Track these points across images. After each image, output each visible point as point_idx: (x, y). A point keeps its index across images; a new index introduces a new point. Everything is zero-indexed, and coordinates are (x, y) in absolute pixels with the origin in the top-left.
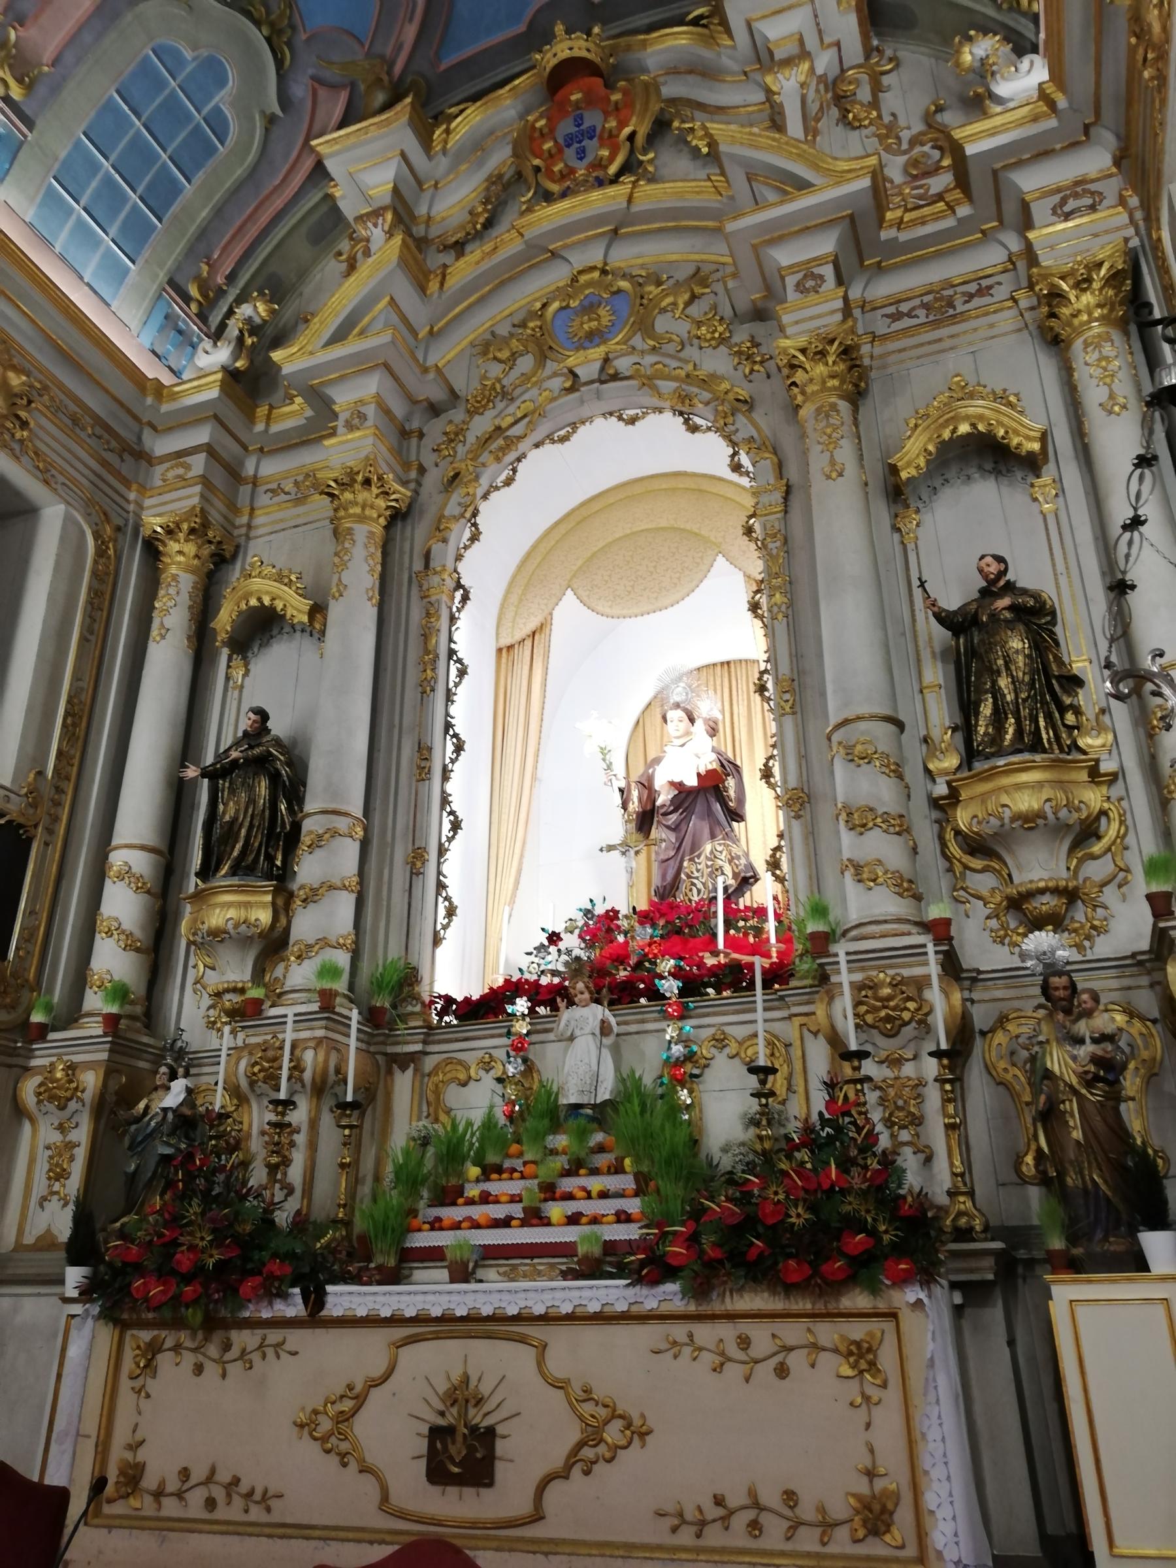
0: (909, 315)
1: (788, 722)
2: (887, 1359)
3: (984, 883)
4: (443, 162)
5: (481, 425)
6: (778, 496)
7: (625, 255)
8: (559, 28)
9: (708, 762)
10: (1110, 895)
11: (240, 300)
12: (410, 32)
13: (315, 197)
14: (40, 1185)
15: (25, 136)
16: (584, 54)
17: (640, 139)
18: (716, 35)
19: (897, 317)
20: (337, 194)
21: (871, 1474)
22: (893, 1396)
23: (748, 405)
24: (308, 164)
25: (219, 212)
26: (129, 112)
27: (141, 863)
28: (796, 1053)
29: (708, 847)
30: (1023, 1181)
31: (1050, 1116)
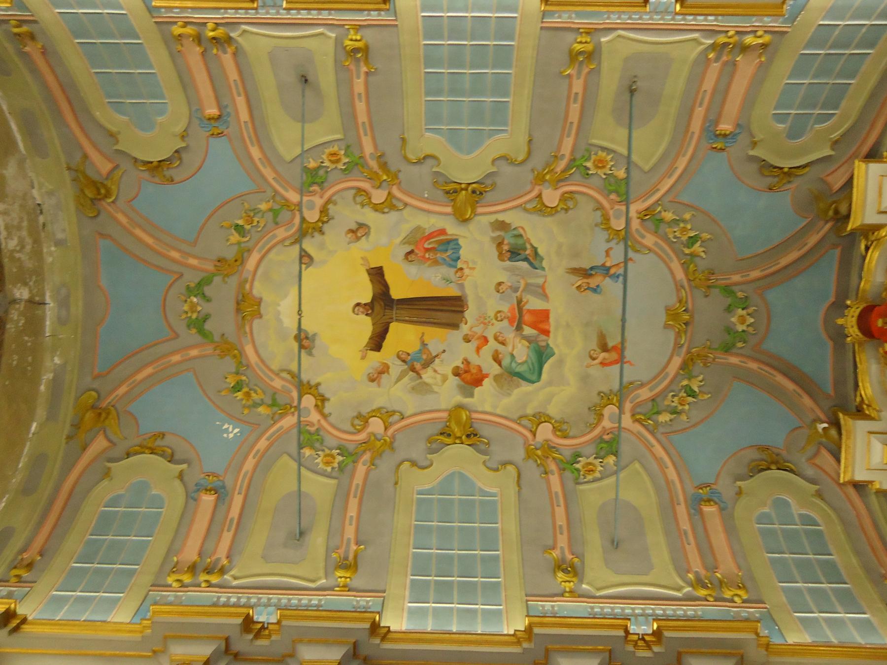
8: (840, 321)
12: (807, 401)
13: (873, 499)
15: (766, 608)
16: (859, 310)
18: (878, 238)
20: (878, 486)
24: (851, 491)
25: (858, 553)
26: (779, 556)
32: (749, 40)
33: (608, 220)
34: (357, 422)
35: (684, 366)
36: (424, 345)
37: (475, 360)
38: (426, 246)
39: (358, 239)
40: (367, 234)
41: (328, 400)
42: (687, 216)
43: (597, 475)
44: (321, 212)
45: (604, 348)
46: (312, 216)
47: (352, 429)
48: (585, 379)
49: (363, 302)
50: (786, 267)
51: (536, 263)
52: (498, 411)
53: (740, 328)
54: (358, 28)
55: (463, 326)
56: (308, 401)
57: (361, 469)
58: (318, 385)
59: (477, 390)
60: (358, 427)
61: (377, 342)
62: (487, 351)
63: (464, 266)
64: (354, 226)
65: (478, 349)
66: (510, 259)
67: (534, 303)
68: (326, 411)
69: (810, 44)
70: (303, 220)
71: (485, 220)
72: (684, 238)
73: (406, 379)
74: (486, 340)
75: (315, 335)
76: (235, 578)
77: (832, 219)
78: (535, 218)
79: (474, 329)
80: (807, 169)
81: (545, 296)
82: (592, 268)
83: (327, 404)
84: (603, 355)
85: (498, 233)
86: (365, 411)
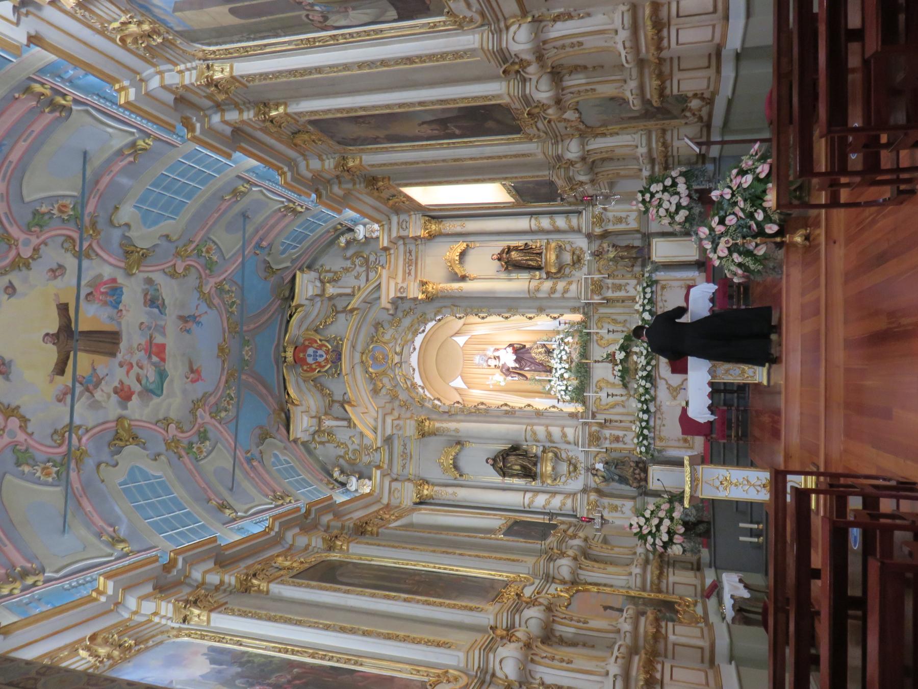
0: (410, 270)
1: (520, 310)
2: (663, 283)
3: (567, 271)
4: (303, 402)
5: (403, 396)
6: (455, 308)
7: (359, 348)
9: (510, 350)
10: (574, 246)
11: (332, 476)
14: (618, 514)
16: (293, 349)
17: (322, 338)
19: (409, 274)
21: (682, 287)
22: (670, 283)
23: (424, 314)
27: (529, 495)
28: (602, 315)
29: (533, 355)
30: (632, 271)
31: (622, 258)
32: (299, 209)
33: (202, 286)
34: (56, 437)
35: (227, 382)
36: (94, 369)
37: (127, 382)
38: (102, 290)
39: (55, 277)
40: (63, 274)
41: (29, 420)
42: (234, 289)
43: (205, 454)
44: (34, 250)
45: (192, 371)
46: (26, 253)
47: (55, 445)
48: (184, 392)
49: (51, 332)
50: (263, 323)
51: (163, 311)
52: (144, 419)
53: (246, 358)
54: (157, 139)
55: (118, 355)
56: (14, 422)
57: (73, 475)
58: (18, 407)
59: (130, 404)
60: (58, 442)
61: (60, 369)
62: (133, 373)
63: (123, 309)
64: (55, 266)
65: (128, 373)
66: (151, 306)
67: (159, 339)
68: (29, 430)
69: (313, 217)
70: (19, 254)
71: (142, 276)
72: (230, 302)
73: (83, 399)
74: (131, 366)
75: (11, 361)
76: (57, 571)
77: (282, 299)
78: (168, 279)
79: (126, 357)
80: (279, 272)
81: (164, 334)
82: (189, 317)
83: (29, 425)
84: (192, 375)
85: (147, 286)
86: (59, 427)
